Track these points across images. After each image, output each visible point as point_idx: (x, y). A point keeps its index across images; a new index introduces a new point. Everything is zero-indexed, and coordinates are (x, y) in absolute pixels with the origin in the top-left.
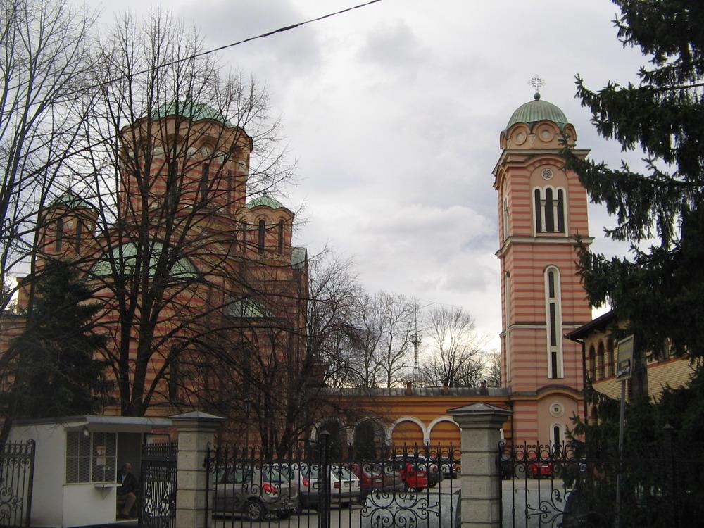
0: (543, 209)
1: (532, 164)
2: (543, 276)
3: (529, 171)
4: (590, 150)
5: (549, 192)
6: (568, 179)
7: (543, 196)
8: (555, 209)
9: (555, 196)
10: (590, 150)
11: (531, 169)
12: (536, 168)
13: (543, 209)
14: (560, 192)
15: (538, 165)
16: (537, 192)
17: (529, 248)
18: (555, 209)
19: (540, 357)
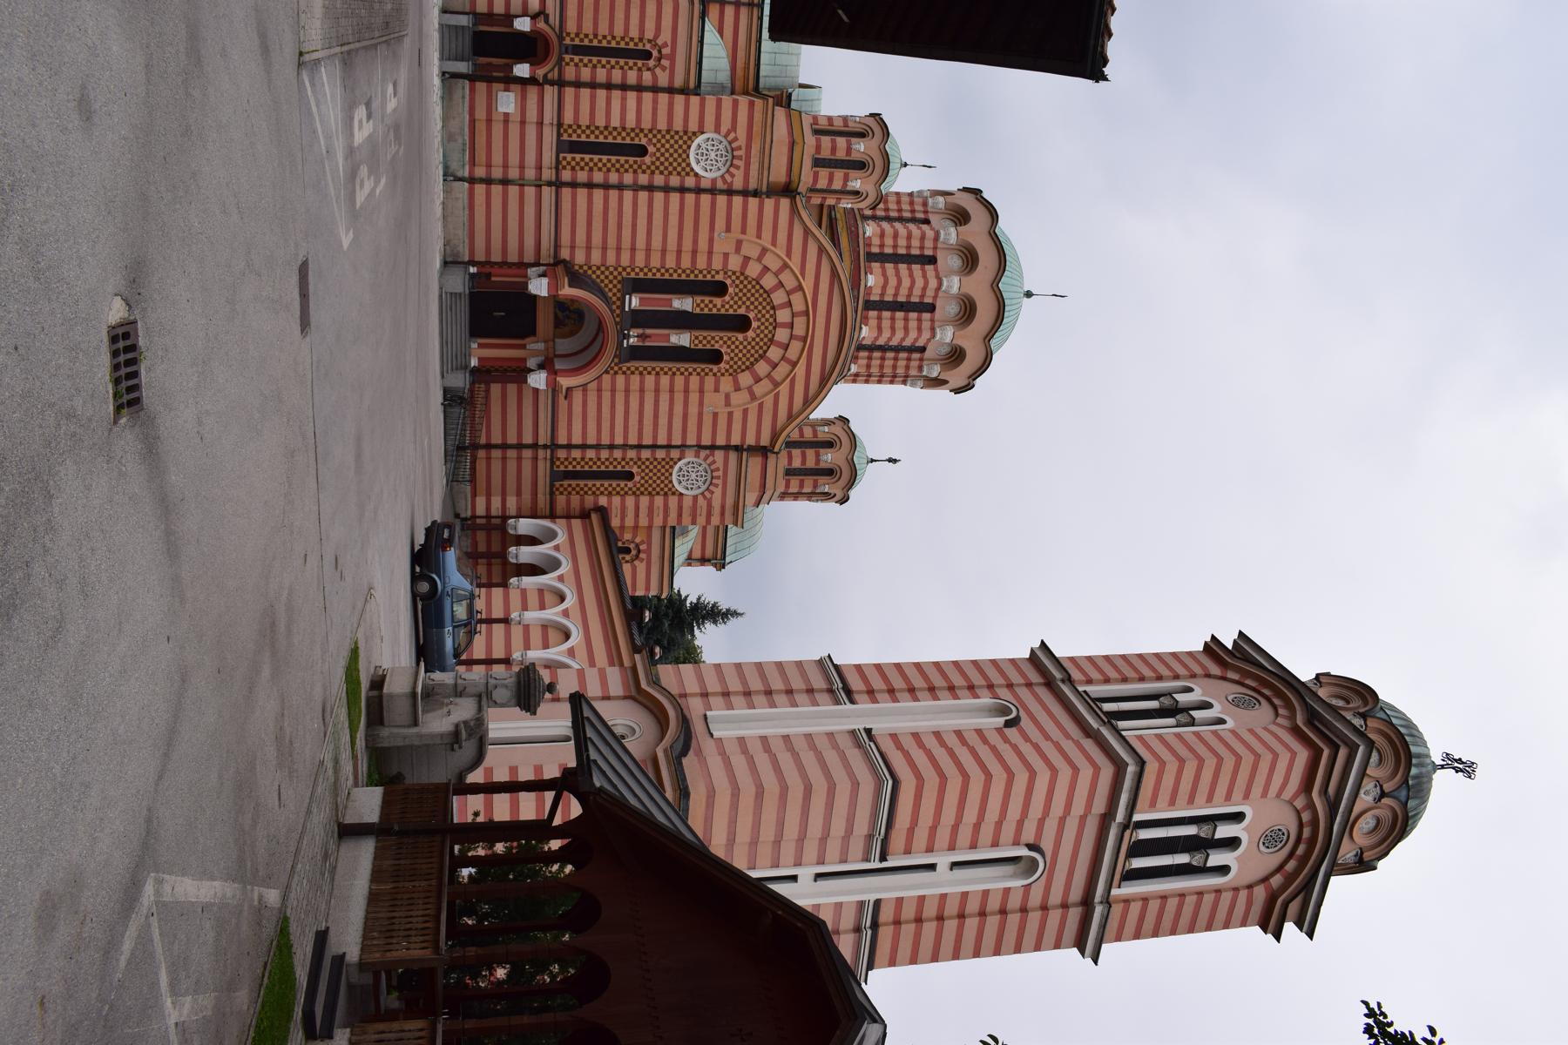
0: (1191, 830)
1: (1311, 806)
2: (1016, 843)
3: (1295, 796)
4: (1310, 935)
5: (1232, 843)
6: (1250, 887)
7: (1224, 831)
8: (1182, 859)
9: (1216, 859)
10: (1310, 935)
11: (1299, 803)
12: (1298, 813)
13: (1191, 830)
14: (1223, 870)
15: (1306, 817)
16: (1238, 817)
17: (1099, 806)
18: (1182, 859)
19: (788, 850)
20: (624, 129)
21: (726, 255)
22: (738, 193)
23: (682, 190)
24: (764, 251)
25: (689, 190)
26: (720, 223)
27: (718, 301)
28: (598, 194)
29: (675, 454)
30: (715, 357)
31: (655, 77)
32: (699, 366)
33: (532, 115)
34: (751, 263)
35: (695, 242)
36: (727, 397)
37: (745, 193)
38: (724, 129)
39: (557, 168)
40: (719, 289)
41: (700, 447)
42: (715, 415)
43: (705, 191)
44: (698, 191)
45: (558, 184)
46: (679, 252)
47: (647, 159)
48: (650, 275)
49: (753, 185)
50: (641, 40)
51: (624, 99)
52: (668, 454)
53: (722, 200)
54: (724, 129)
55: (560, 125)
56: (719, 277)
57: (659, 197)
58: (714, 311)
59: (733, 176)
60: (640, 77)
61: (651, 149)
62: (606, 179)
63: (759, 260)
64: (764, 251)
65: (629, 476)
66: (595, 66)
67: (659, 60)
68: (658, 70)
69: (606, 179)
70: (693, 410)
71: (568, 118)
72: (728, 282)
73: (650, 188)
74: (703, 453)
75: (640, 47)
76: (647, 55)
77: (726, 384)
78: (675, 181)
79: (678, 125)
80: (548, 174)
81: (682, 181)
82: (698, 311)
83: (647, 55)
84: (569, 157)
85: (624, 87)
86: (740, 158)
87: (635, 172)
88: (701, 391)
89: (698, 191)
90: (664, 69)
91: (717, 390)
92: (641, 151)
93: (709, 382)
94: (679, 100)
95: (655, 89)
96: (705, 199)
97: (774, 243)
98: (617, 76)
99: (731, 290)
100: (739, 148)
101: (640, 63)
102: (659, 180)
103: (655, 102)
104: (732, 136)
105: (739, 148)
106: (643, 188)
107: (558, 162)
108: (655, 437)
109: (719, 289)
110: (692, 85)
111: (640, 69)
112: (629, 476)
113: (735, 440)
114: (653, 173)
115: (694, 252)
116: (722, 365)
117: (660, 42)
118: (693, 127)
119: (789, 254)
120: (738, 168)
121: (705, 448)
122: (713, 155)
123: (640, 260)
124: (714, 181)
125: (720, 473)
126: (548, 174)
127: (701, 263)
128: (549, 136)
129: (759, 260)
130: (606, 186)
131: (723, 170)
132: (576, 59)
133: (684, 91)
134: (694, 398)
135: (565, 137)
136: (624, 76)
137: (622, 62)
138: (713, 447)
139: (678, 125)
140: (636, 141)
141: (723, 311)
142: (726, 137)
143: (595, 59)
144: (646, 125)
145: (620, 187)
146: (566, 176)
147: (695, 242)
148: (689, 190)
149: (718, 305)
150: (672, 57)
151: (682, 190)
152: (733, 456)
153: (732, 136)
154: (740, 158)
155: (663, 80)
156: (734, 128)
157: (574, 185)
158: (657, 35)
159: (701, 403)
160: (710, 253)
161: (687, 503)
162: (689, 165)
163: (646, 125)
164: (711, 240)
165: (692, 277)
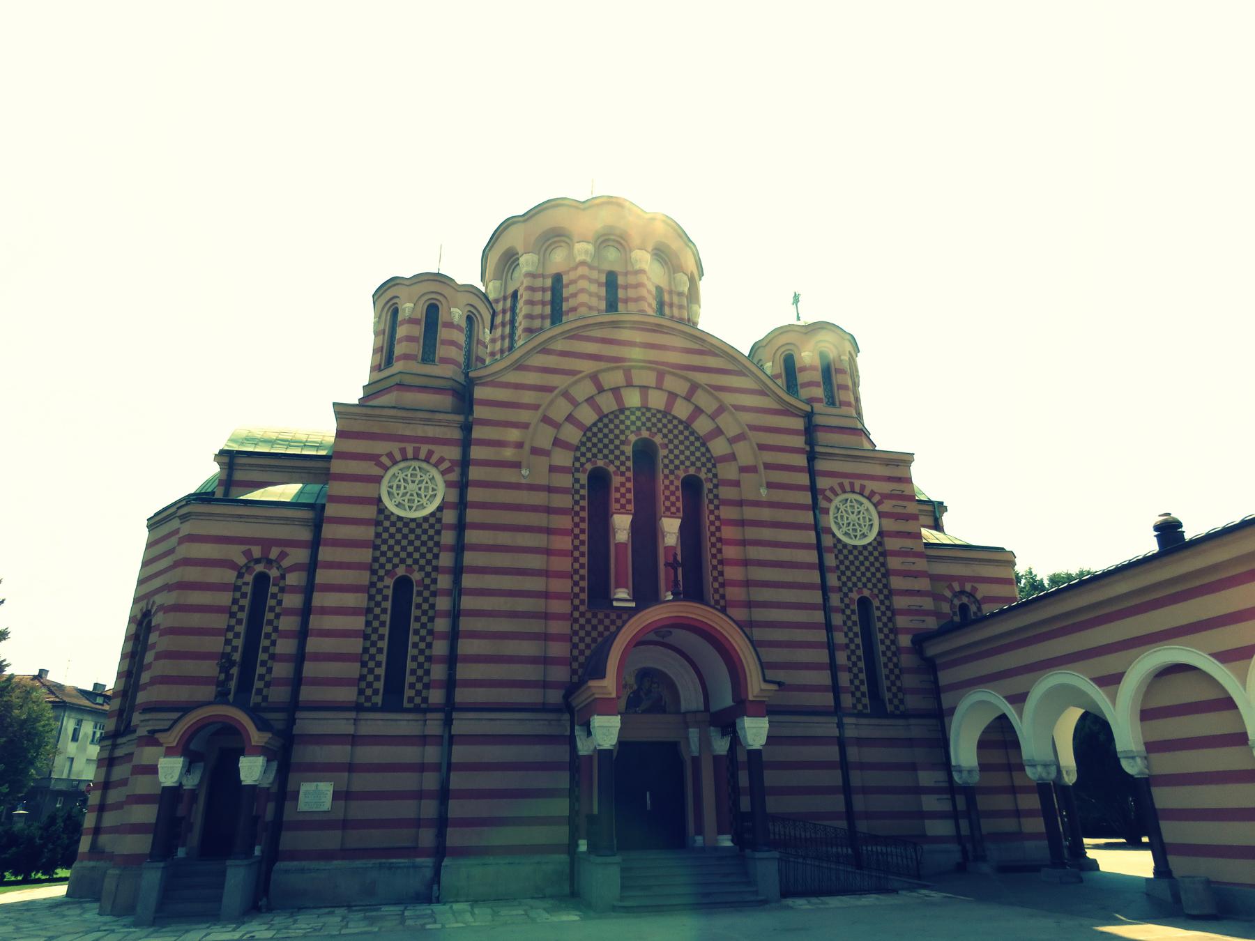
20: (369, 611)
21: (553, 469)
22: (465, 453)
23: (461, 527)
24: (546, 420)
25: (461, 517)
26: (508, 475)
27: (616, 481)
28: (466, 647)
29: (827, 541)
30: (692, 487)
31: (294, 568)
32: (707, 507)
33: (339, 753)
34: (561, 437)
35: (534, 509)
36: (744, 469)
37: (466, 443)
38: (376, 471)
39: (425, 711)
40: (599, 481)
41: (814, 506)
42: (770, 485)
43: (462, 495)
44: (462, 505)
45: (449, 708)
46: (549, 531)
47: (416, 576)
48: (584, 572)
49: (457, 434)
50: (237, 588)
51: (324, 611)
52: (829, 550)
53: (475, 473)
54: (376, 471)
55: (358, 708)
56: (584, 479)
57: (469, 558)
58: (630, 485)
59: (442, 460)
60: (293, 589)
61: (401, 571)
62: (442, 636)
63: (557, 426)
64: (546, 420)
65: (864, 603)
66: (273, 657)
67: (269, 562)
68: (286, 563)
69: (442, 636)
70: (766, 514)
71: (347, 694)
72: (589, 466)
73: (458, 571)
74: (823, 503)
75: (248, 589)
76: (262, 581)
77: (728, 471)
78: (448, 538)
79: (368, 533)
80: (434, 725)
81: (449, 527)
82: (630, 507)
83: (262, 581)
84: (409, 693)
85: (306, 611)
86: (416, 451)
87: (434, 594)
88: (740, 503)
89: (462, 505)
90: (283, 555)
91: (736, 484)
92: (403, 585)
93: (726, 493)
94: (328, 531)
95: (312, 566)
96: (473, 495)
97: (536, 407)
98: (288, 623)
99: (600, 463)
100: (403, 451)
101: (273, 589)
102: (446, 560)
103: (331, 565)
104: (385, 460)
105: (403, 451)
106: (457, 581)
107: (416, 709)
108: (809, 566)
109: (599, 481)
110: (308, 514)
111: (282, 590)
112: (864, 603)
113: (801, 461)
114: (436, 569)
115: (549, 510)
116: (703, 476)
117: (241, 561)
118: (370, 512)
119: (549, 389)
120: (430, 453)
121: (815, 499)
122: (412, 487)
123: (563, 585)
124: (449, 484)
125: (846, 482)
126: (434, 725)
127: (564, 501)
128: (375, 724)
129: (557, 426)
130: (454, 636)
131: (434, 472)
132: (258, 684)
133: (317, 526)
134: (750, 513)
135: (378, 699)
136: (290, 612)
137: (269, 616)
138: (813, 489)
139: (368, 533)
140: (389, 592)
141: (630, 474)
142: (387, 469)
143: (262, 656)
144: (364, 578)
145: (455, 614)
146: (436, 696)
147: (534, 509)
148: (461, 517)
149: (622, 483)
150: (267, 544)
151: (461, 527)
152: (821, 465)
153: (385, 460)
154: (416, 451)
155: (300, 556)
156: (374, 458)
157: (450, 684)
158: (230, 564)
159: (757, 504)
160: (550, 489)
161: (890, 525)
162: (425, 519)
163: (364, 578)
164: (532, 488)
165: (584, 514)
